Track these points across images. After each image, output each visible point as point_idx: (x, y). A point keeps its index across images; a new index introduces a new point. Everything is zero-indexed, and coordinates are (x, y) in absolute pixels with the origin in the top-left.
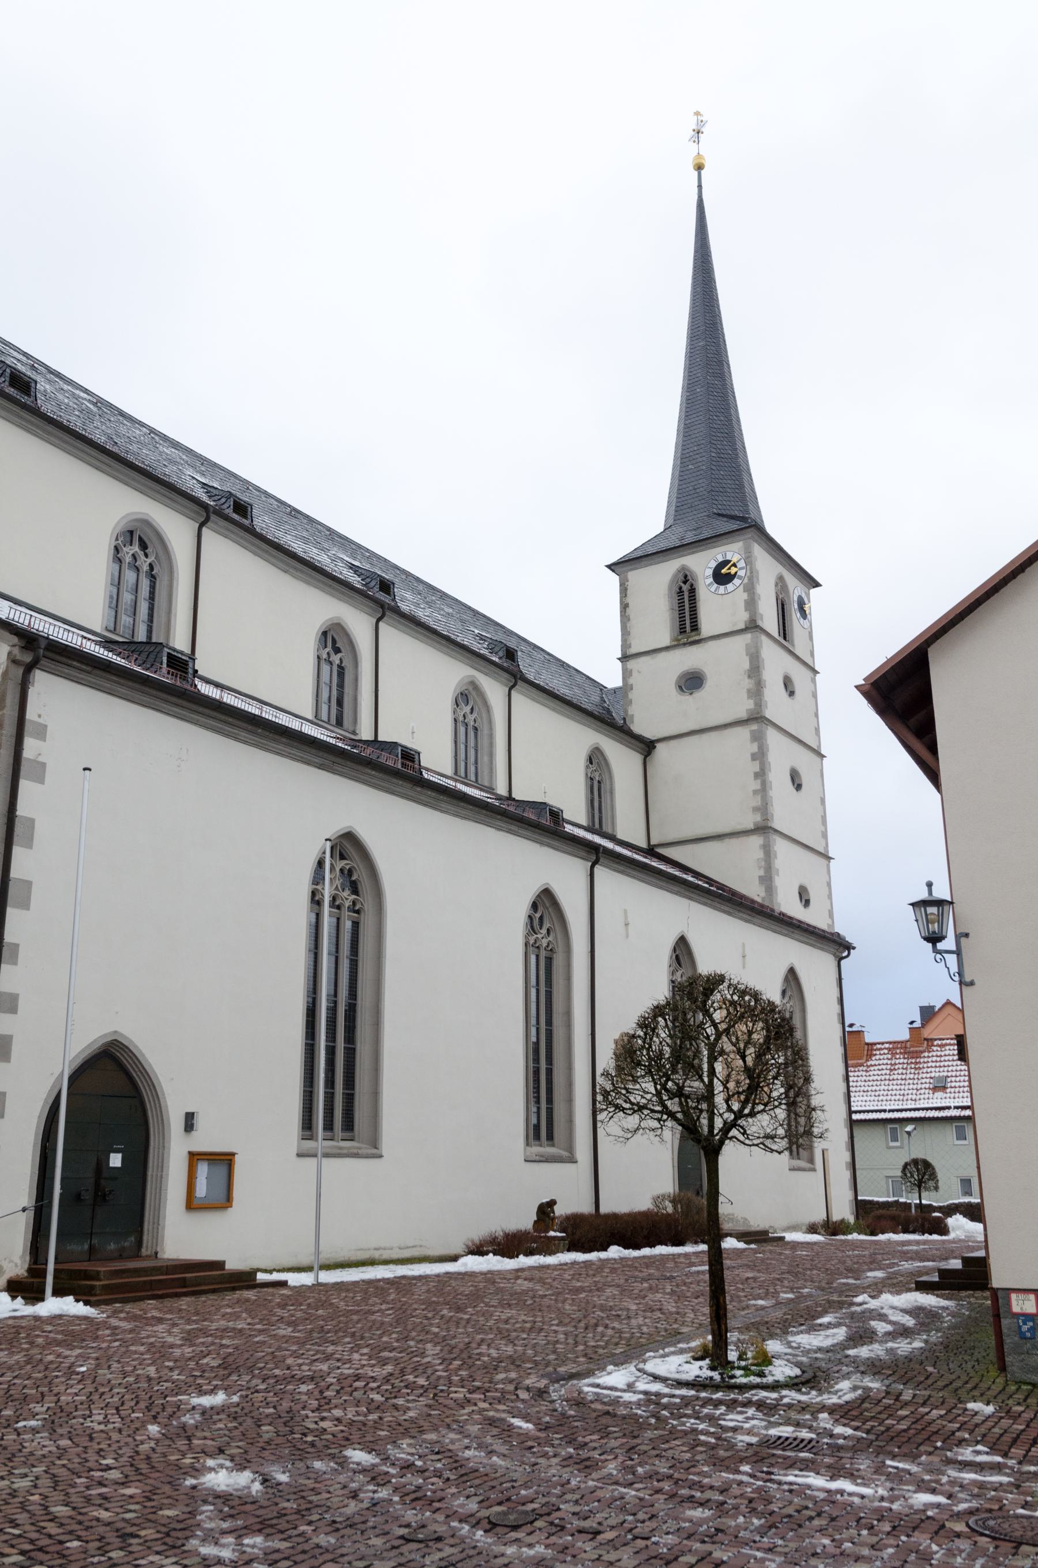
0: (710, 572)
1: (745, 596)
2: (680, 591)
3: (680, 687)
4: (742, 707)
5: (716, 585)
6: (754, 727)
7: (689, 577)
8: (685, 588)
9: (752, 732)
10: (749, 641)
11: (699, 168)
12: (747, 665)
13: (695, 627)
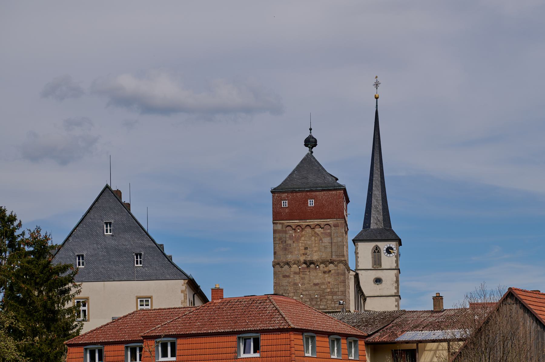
0: (385, 249)
1: (395, 259)
2: (375, 252)
4: (393, 291)
5: (387, 254)
6: (397, 298)
7: (378, 248)
9: (396, 299)
10: (396, 272)
12: (395, 280)
13: (381, 265)
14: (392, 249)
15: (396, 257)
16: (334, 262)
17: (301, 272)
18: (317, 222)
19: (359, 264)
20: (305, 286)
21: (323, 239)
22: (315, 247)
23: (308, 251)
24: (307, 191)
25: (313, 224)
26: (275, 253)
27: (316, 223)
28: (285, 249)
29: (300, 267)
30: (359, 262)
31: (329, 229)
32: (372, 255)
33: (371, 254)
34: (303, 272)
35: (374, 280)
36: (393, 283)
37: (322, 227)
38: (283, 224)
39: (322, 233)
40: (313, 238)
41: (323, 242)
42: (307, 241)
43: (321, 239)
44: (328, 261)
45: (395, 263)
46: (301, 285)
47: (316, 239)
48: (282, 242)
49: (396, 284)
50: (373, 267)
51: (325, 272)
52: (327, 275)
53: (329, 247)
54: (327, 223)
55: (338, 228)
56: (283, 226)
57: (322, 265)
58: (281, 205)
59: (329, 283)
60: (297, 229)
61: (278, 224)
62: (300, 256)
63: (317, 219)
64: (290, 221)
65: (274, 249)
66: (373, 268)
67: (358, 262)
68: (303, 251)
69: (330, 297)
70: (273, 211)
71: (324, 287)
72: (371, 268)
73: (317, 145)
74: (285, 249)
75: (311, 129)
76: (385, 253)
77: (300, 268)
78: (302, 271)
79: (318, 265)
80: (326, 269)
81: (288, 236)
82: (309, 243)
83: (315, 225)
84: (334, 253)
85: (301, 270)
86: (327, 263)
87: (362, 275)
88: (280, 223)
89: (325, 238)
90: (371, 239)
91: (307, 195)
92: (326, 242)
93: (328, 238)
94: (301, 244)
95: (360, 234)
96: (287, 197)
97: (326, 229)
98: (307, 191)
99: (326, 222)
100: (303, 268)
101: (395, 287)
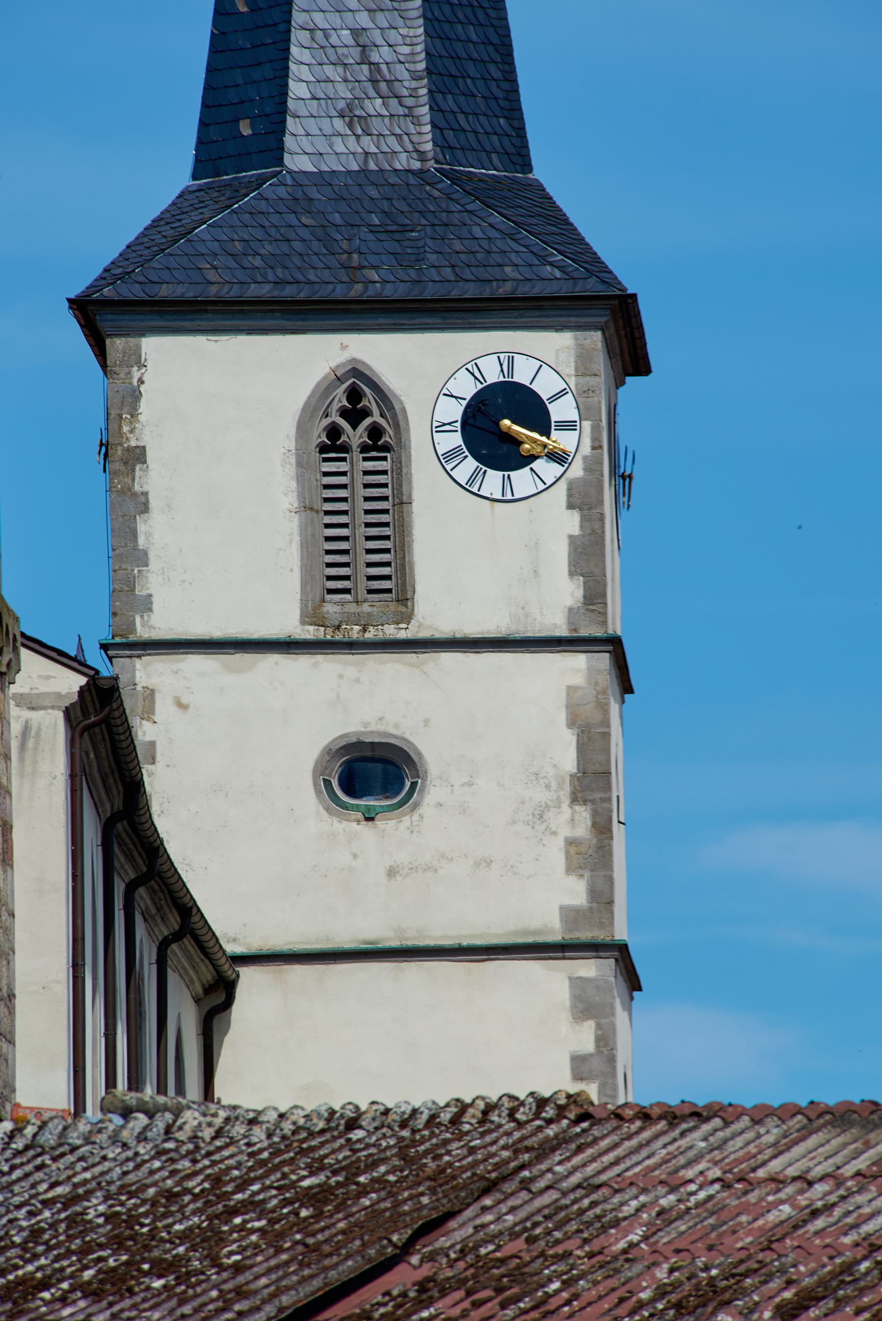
1: (572, 523)
3: (327, 783)
5: (471, 464)
7: (369, 400)
10: (579, 680)
12: (569, 762)
35: (320, 770)
36: (540, 796)
45: (572, 574)
49: (584, 814)
50: (318, 620)
66: (310, 633)
67: (143, 558)
76: (451, 455)
87: (182, 706)
90: (289, 292)
101: (571, 842)
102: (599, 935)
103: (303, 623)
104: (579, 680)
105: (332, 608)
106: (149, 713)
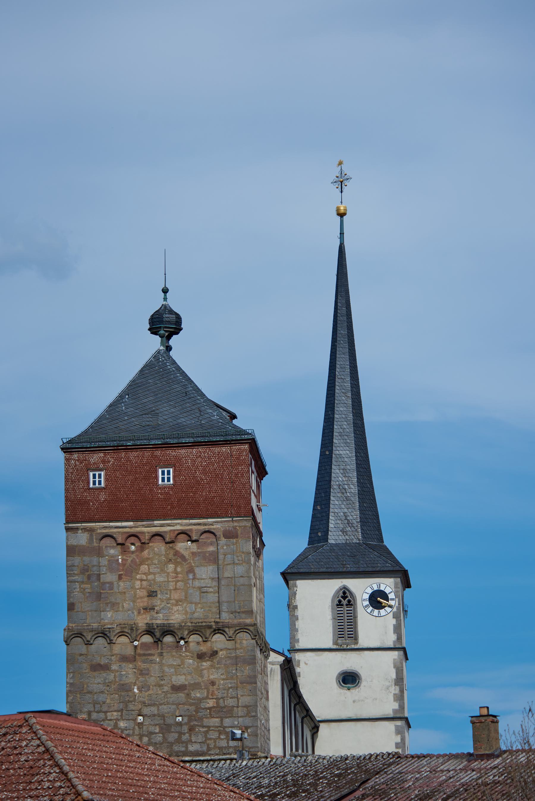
0: (367, 596)
1: (394, 621)
2: (340, 604)
3: (339, 681)
5: (371, 608)
6: (399, 723)
7: (348, 594)
8: (345, 602)
9: (396, 726)
10: (396, 657)
11: (342, 215)
12: (394, 676)
14: (385, 596)
15: (396, 616)
16: (227, 630)
17: (140, 655)
18: (181, 525)
19: (300, 636)
20: (150, 692)
21: (197, 570)
22: (176, 589)
23: (156, 602)
24: (156, 447)
25: (171, 531)
26: (71, 607)
27: (179, 527)
28: (99, 597)
29: (136, 643)
30: (300, 632)
31: (211, 544)
32: (332, 612)
33: (330, 610)
34: (144, 655)
36: (388, 684)
37: (194, 538)
38: (91, 530)
39: (193, 554)
40: (171, 567)
41: (198, 576)
42: (154, 574)
43: (191, 570)
44: (210, 627)
45: (394, 633)
46: (138, 689)
47: (179, 569)
48: (89, 577)
49: (398, 688)
50: (337, 645)
51: (201, 656)
52: (206, 664)
53: (211, 590)
54: (206, 528)
55: (235, 540)
56: (91, 536)
57: (194, 638)
58: (89, 483)
59: (213, 683)
60: (128, 544)
61: (80, 531)
62: (136, 613)
63: (181, 518)
64: (112, 524)
65: (69, 597)
66: (335, 647)
67: (297, 630)
68: (145, 602)
69: (215, 721)
70: (67, 499)
71: (198, 695)
72: (330, 645)
73: (181, 329)
74: (99, 597)
75: (165, 291)
76: (366, 606)
77: (136, 647)
78: (142, 652)
79: (182, 638)
80: (204, 648)
81: (104, 561)
82: (160, 579)
83: (177, 532)
84: (225, 604)
85: (139, 651)
86: (208, 632)
87: (306, 664)
88: (85, 529)
89: (202, 568)
90: (329, 570)
91: (154, 457)
92: (204, 576)
93: (211, 568)
94: (138, 584)
95: (302, 557)
96: (103, 462)
97: (205, 543)
98: (156, 447)
99: (205, 524)
100: (144, 645)
101: (395, 694)
102: (401, 715)
103: (333, 644)
104: (396, 657)
105: (340, 641)
106: (299, 665)
